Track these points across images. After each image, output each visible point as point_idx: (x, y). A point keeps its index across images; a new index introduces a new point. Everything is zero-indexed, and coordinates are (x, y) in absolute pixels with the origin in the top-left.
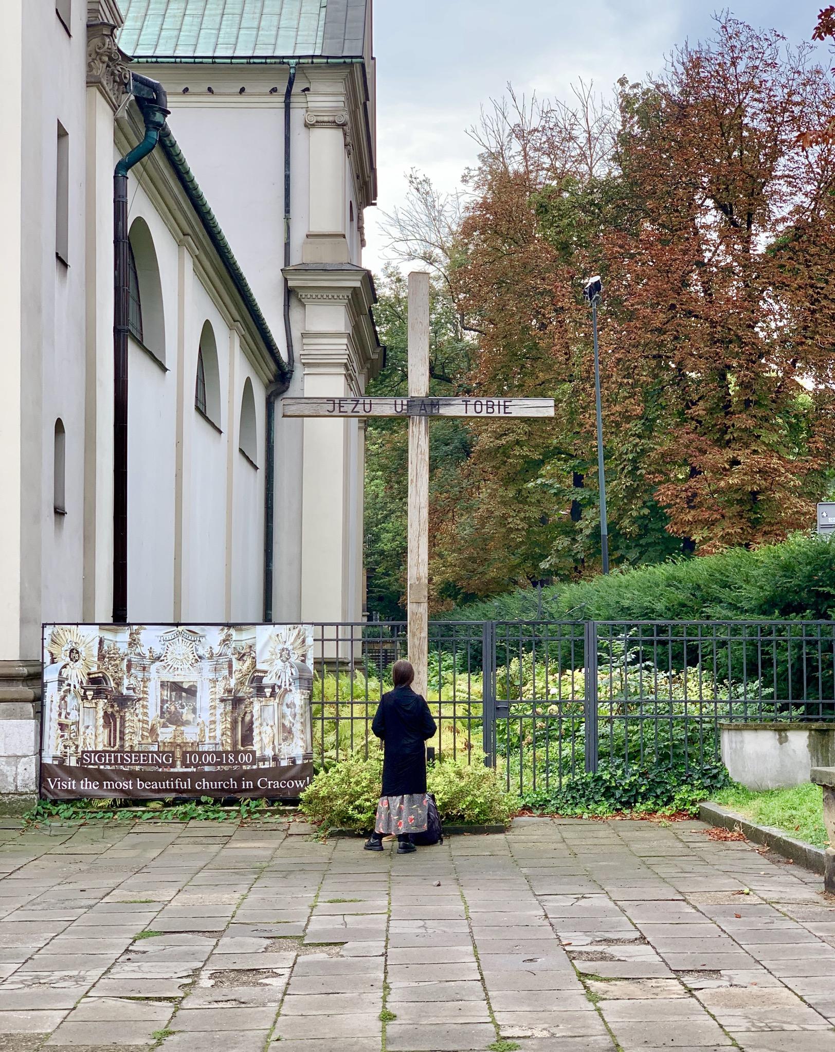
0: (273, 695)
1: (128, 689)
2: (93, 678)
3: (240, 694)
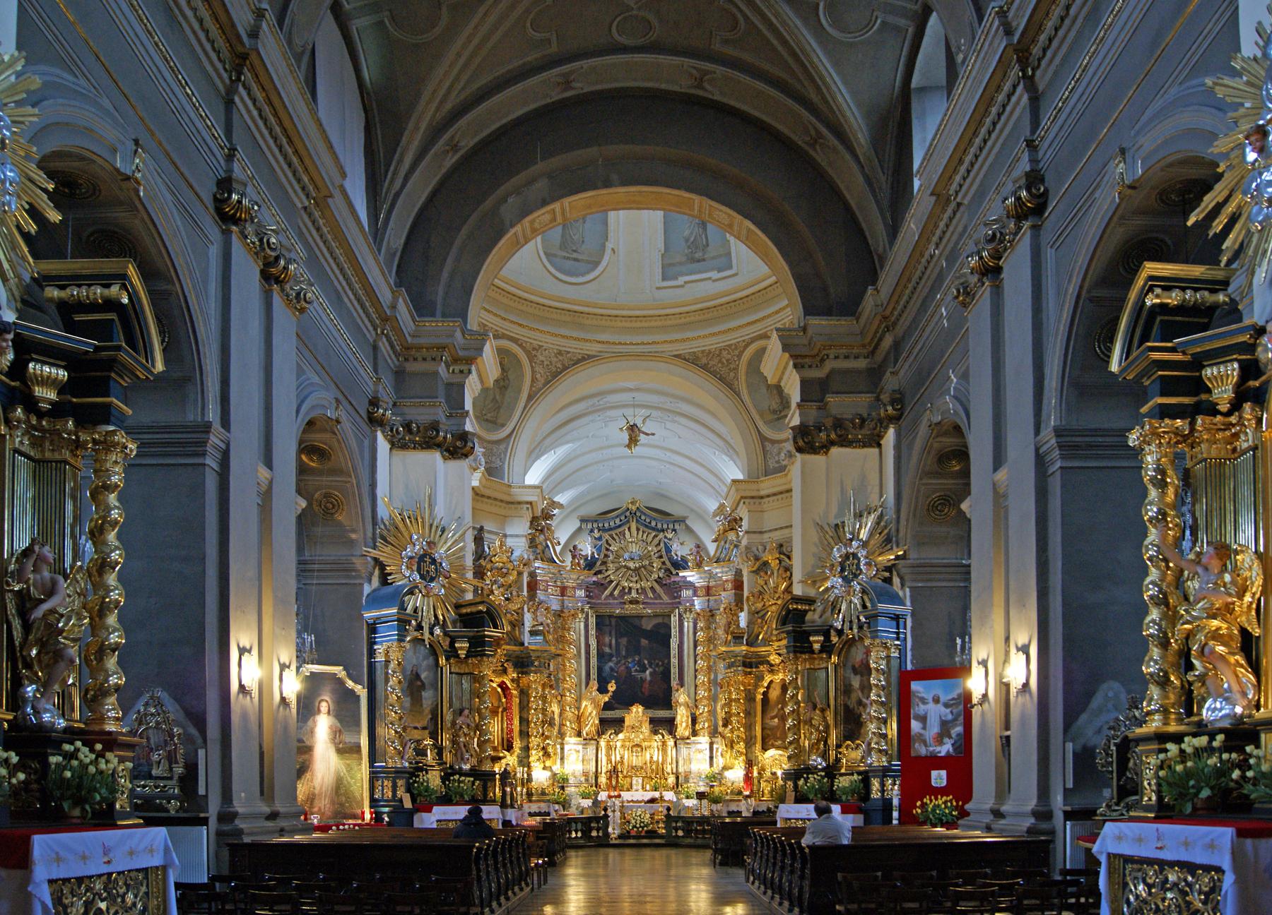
0: (827, 648)
2: (467, 614)
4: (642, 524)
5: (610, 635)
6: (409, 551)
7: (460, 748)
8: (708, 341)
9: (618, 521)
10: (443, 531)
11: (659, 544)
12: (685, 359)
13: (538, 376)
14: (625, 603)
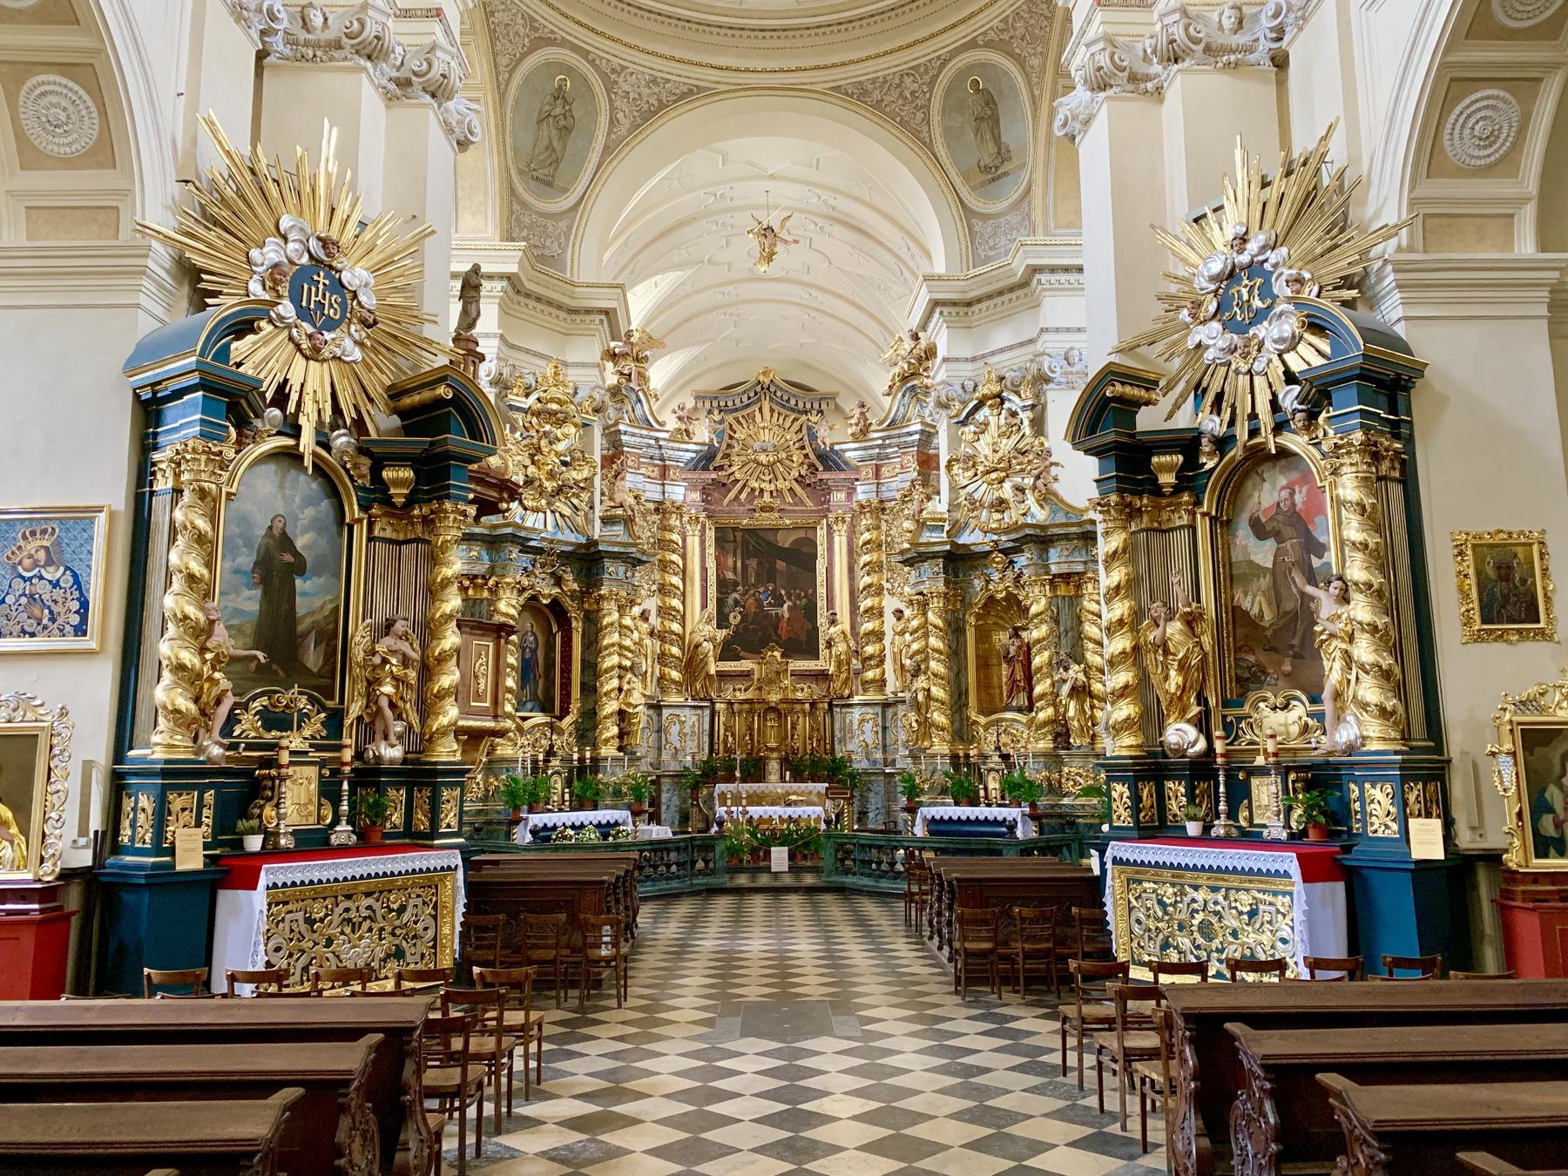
0: (1190, 479)
1: (607, 521)
4: (778, 403)
5: (735, 556)
6: (269, 253)
7: (379, 710)
8: (882, 63)
9: (745, 398)
10: (363, 225)
11: (800, 430)
12: (846, 94)
13: (620, 116)
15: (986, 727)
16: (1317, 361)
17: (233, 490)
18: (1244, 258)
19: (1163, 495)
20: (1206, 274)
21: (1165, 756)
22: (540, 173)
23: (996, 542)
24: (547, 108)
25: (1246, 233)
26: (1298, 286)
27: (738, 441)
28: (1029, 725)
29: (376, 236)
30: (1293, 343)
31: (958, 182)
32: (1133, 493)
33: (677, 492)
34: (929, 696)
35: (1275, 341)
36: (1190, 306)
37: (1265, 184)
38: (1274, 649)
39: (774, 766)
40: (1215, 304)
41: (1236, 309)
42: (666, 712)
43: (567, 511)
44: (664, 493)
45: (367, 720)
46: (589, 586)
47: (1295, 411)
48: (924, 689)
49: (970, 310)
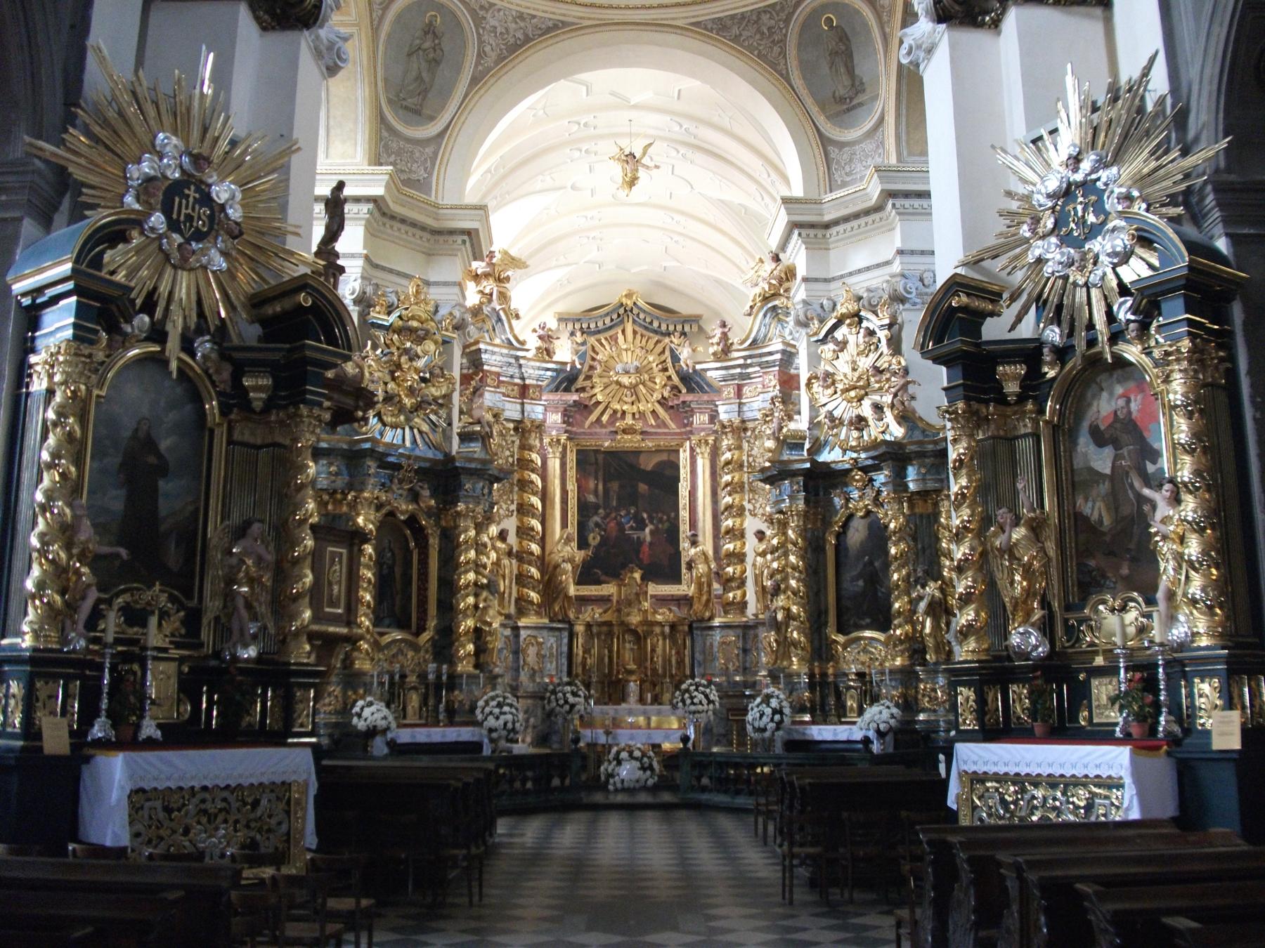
0: (1033, 385)
1: (465, 437)
2: (276, 318)
3: (829, 456)
4: (640, 325)
5: (596, 479)
7: (235, 608)
9: (608, 320)
11: (663, 352)
12: (706, 29)
13: (488, 49)
14: (616, 432)
15: (845, 647)
16: (1146, 272)
17: (103, 393)
18: (1079, 177)
19: (1008, 404)
20: (1043, 191)
21: (1009, 658)
22: (410, 102)
23: (855, 460)
24: (418, 42)
25: (1079, 153)
26: (1127, 203)
27: (600, 362)
28: (886, 644)
29: (244, 153)
30: (1124, 257)
31: (814, 110)
32: (980, 401)
33: (536, 411)
34: (789, 616)
35: (1109, 255)
36: (1029, 221)
37: (1095, 109)
38: (1111, 553)
39: (633, 687)
40: (1052, 220)
41: (1072, 225)
42: (523, 633)
43: (425, 428)
44: (523, 412)
45: (223, 620)
46: (445, 502)
47: (1129, 321)
48: (783, 608)
49: (828, 232)
